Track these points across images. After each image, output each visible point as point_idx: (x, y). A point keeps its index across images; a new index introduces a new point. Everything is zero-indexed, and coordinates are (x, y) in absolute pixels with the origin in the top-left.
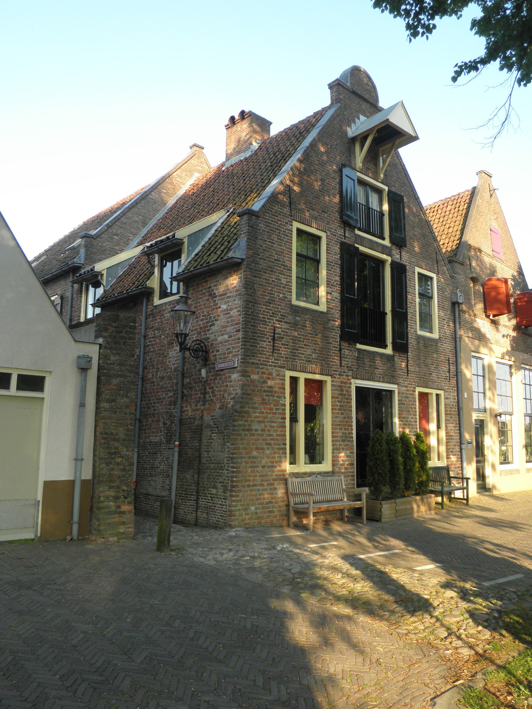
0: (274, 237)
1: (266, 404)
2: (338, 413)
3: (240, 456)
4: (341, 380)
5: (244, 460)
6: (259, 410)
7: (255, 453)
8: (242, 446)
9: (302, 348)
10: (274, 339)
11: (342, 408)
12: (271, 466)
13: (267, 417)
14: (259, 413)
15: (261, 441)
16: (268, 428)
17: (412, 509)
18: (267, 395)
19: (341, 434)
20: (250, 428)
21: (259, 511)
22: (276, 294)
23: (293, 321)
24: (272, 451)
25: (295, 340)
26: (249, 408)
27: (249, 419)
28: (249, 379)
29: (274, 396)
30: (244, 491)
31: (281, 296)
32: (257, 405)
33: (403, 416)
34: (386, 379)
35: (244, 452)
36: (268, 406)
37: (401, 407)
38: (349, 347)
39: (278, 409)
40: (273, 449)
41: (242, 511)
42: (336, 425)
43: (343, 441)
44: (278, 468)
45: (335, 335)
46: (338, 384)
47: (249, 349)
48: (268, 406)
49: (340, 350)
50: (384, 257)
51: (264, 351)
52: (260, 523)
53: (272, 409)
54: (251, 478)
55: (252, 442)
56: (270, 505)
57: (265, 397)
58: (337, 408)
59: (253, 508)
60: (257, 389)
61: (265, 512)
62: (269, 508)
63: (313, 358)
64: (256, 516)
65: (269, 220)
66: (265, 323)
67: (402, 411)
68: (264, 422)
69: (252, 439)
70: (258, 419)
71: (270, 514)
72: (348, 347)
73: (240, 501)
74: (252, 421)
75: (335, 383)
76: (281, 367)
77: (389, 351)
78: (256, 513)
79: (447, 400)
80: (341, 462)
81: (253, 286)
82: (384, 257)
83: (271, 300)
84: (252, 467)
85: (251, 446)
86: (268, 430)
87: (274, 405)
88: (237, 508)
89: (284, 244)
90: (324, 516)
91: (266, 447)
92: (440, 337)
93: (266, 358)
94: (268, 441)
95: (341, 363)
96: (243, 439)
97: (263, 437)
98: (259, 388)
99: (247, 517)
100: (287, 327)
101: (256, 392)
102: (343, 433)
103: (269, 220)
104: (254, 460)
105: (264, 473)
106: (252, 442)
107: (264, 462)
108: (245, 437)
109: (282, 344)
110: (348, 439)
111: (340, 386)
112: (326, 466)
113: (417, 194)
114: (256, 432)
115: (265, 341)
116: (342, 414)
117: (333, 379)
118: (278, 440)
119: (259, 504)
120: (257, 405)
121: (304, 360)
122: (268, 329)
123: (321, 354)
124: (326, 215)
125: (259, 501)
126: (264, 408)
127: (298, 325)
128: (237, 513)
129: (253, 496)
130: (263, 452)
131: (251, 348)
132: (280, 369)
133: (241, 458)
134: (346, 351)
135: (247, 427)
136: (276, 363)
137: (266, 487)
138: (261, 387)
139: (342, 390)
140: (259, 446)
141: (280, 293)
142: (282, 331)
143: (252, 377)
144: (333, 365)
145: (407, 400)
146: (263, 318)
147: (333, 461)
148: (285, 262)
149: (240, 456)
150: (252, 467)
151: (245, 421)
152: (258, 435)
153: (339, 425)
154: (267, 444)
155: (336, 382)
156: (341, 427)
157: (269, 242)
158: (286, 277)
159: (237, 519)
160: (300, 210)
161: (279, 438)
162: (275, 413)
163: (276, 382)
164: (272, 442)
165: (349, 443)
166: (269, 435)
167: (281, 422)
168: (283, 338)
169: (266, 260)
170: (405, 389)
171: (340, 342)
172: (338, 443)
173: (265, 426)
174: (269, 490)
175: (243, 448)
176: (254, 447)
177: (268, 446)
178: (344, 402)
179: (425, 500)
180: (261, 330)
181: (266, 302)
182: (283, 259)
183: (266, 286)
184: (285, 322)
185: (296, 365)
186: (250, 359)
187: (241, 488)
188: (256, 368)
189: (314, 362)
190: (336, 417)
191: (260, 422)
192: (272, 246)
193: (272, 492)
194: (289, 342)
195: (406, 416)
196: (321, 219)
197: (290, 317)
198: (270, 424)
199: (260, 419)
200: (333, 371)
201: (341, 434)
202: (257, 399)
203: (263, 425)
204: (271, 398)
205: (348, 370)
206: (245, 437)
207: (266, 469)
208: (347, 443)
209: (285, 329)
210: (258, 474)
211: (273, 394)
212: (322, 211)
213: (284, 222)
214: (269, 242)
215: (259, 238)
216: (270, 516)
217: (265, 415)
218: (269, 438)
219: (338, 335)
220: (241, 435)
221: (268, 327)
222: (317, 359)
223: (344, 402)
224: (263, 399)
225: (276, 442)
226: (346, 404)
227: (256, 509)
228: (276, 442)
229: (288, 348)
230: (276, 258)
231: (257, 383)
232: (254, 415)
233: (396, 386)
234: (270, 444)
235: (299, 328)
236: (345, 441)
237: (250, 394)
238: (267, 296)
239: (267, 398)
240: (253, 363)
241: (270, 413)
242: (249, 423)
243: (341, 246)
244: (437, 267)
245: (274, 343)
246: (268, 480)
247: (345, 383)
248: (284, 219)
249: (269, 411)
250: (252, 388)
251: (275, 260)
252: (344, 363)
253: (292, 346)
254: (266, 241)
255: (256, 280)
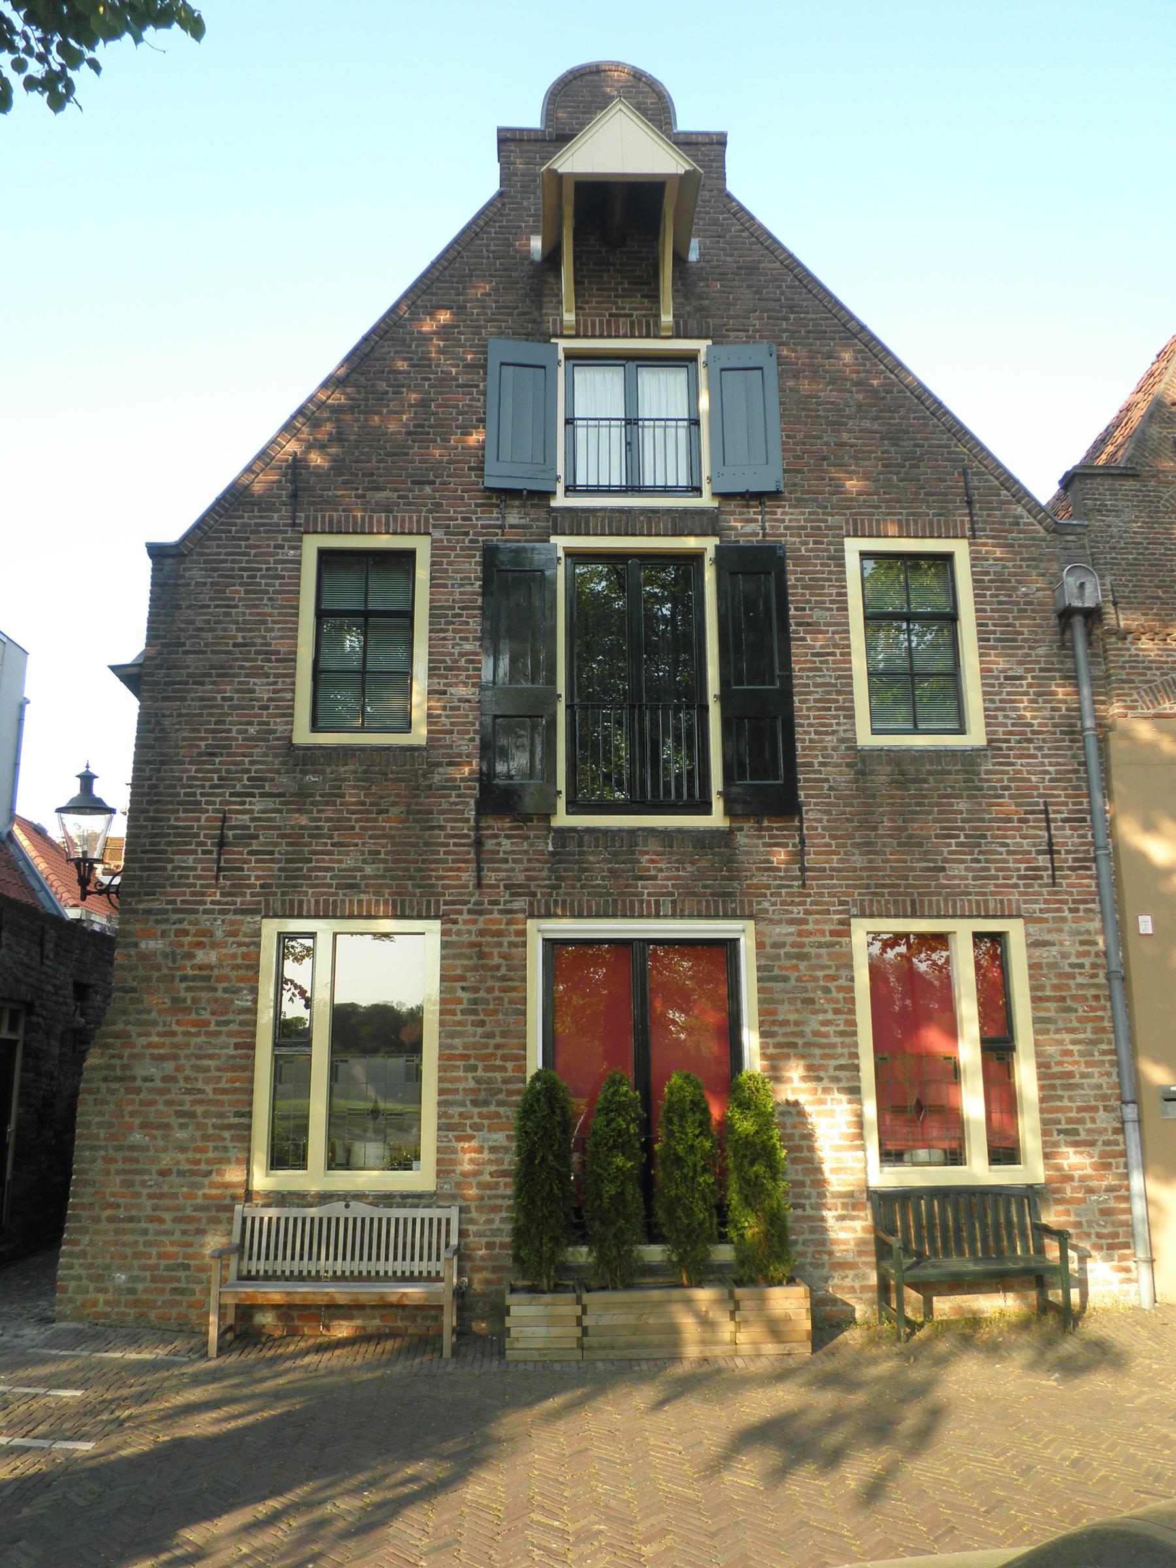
0: (237, 592)
1: (188, 1010)
2: (459, 1023)
3: (90, 1142)
4: (481, 925)
5: (103, 1153)
6: (161, 1029)
7: (137, 1137)
8: (97, 1119)
9: (322, 853)
10: (222, 843)
11: (479, 1007)
12: (188, 1171)
13: (187, 1045)
14: (159, 1034)
15: (161, 1107)
16: (188, 1073)
17: (674, 1330)
18: (189, 989)
19: (471, 1084)
20: (128, 1073)
21: (140, 1287)
22: (234, 728)
23: (294, 788)
24: (198, 1134)
25: (295, 837)
26: (127, 1023)
27: (127, 1052)
28: (133, 952)
29: (214, 990)
30: (96, 1232)
31: (252, 730)
32: (154, 1015)
33: (781, 1017)
34: (689, 904)
35: (102, 1133)
36: (193, 1016)
37: (770, 990)
38: (517, 828)
39: (227, 1023)
40: (199, 1126)
41: (85, 1282)
42: (451, 1057)
43: (475, 1103)
44: (215, 1178)
45: (456, 804)
46: (465, 938)
47: (140, 878)
48: (193, 1016)
49: (479, 843)
50: (691, 543)
51: (187, 877)
52: (139, 1316)
53: (206, 1023)
54: (121, 1201)
55: (130, 1108)
56: (182, 1274)
57: (183, 994)
58: (459, 1007)
59: (121, 1277)
60: (156, 975)
61: (162, 1290)
62: (179, 1280)
63: (364, 877)
64: (130, 1297)
65: (219, 554)
66: (193, 806)
67: (773, 1001)
68: (175, 1057)
69: (133, 1102)
70: (156, 1051)
71: (179, 1298)
72: (511, 829)
73: (83, 1254)
74: (133, 1056)
75: (454, 938)
76: (243, 912)
77: (716, 819)
78: (132, 1291)
79: (1037, 952)
80: (467, 1167)
81: (158, 723)
82: (691, 543)
83: (216, 747)
84: (124, 1172)
85: (127, 1119)
86: (187, 1079)
87: (213, 1013)
88: (72, 1272)
89: (270, 599)
90: (383, 1317)
91: (174, 1121)
92: (990, 741)
93: (193, 894)
94: (187, 1107)
95: (479, 878)
96: (103, 1102)
97: (168, 1097)
98: (165, 971)
99: (101, 1297)
100: (272, 806)
101: (154, 984)
102: (478, 1081)
103: (219, 554)
104: (135, 1154)
105: (165, 1189)
106: (130, 1108)
107: (166, 1161)
108: (109, 1098)
109: (251, 853)
110: (501, 1097)
111: (472, 945)
112: (421, 1178)
113: (852, 318)
114: (148, 1084)
115: (194, 852)
116: (482, 1023)
117: (449, 926)
118: (219, 1103)
119: (143, 1268)
120: (154, 1015)
121: (330, 886)
122: (204, 822)
123: (396, 861)
124: (428, 489)
125: (143, 1261)
126: (178, 1023)
127: (312, 795)
128: (72, 1285)
129: (124, 1244)
130: (164, 1137)
131: (145, 874)
132: (238, 917)
133: (93, 1148)
134: (505, 842)
135: (119, 1073)
136: (227, 903)
137: (168, 1225)
138: (171, 969)
139: (482, 955)
140: (152, 1120)
141: (250, 723)
142: (253, 820)
143: (143, 945)
144: (445, 887)
145: (803, 965)
146: (186, 794)
147: (439, 1162)
148: (270, 645)
149: (90, 1142)
150: (124, 1172)
151: (113, 1056)
152: (151, 1090)
153: (465, 1057)
154: (181, 1114)
155: (459, 933)
156: (472, 1062)
157: (217, 606)
158: (271, 680)
159: (70, 1300)
160: (329, 503)
161: (225, 1097)
162: (217, 1034)
163: (224, 951)
164: (199, 1109)
165: (501, 1110)
166: (189, 1092)
167: (234, 1057)
168: (256, 837)
169: (204, 652)
170: (792, 929)
171: (477, 821)
172: (454, 1111)
173: (178, 1069)
174: (178, 1233)
175: (100, 1125)
176: (137, 1121)
177: (181, 1120)
178: (490, 990)
179: (747, 1304)
180: (177, 827)
181: (200, 754)
182: (265, 637)
183: (201, 715)
184: (262, 795)
185: (301, 902)
186: (139, 902)
187: (87, 1223)
188: (157, 922)
189: (367, 886)
190: (452, 1035)
191: (161, 1058)
192: (227, 614)
193: (190, 1239)
194: (276, 845)
195: (792, 1017)
196: (410, 504)
197: (284, 780)
198: (193, 1061)
199: (161, 1051)
200: (446, 903)
201: (471, 1084)
202: (156, 1000)
203: (170, 1066)
204: (204, 995)
205: (512, 895)
206: (109, 1098)
207: (174, 1178)
208: (492, 1108)
209: (263, 812)
210: (145, 1191)
211: (213, 983)
212: (413, 483)
213: (269, 546)
214: (217, 606)
215: (184, 604)
216: (179, 1303)
217: (179, 1039)
218: (188, 1098)
219: (472, 801)
220: (98, 1091)
221: (204, 816)
222: (383, 877)
223: (490, 990)
224: (175, 1000)
225: (212, 1109)
226: (496, 993)
227: (132, 1279)
228: (212, 1109)
229: (272, 861)
230: (240, 640)
231: (159, 959)
232: (143, 1040)
233: (750, 924)
234: (192, 1115)
235: (313, 803)
236: (486, 1103)
237: (133, 990)
238: (202, 739)
239: (189, 995)
240: (148, 912)
241: (197, 1035)
242: (125, 1061)
243: (483, 556)
244: (971, 515)
245: (219, 854)
246: (177, 1208)
247: (499, 933)
248: (268, 539)
249: (193, 1030)
250: (141, 972)
251: (235, 645)
252: (490, 878)
253: (287, 853)
254: (209, 606)
255: (168, 708)
